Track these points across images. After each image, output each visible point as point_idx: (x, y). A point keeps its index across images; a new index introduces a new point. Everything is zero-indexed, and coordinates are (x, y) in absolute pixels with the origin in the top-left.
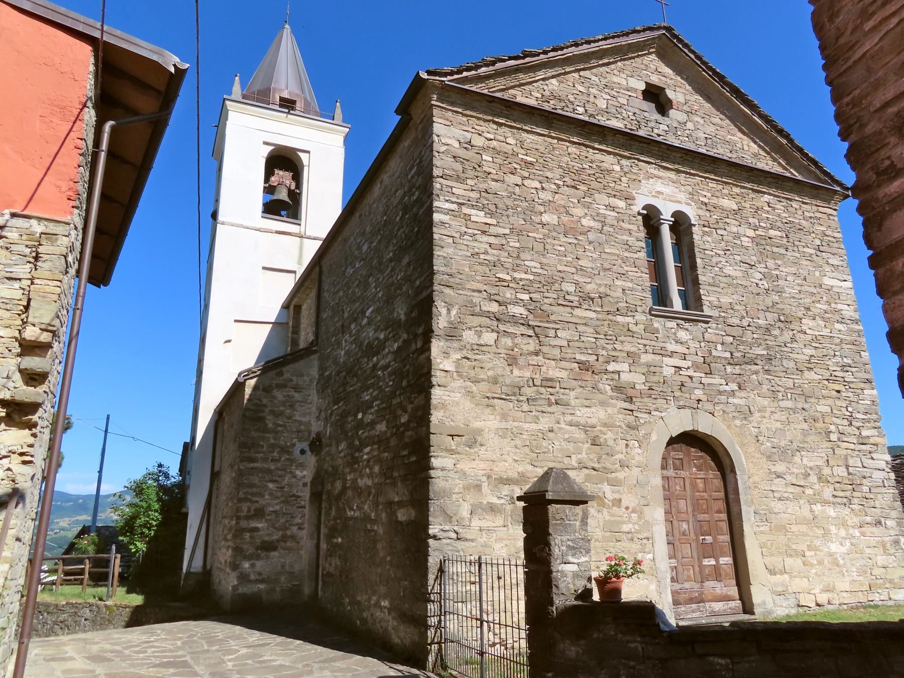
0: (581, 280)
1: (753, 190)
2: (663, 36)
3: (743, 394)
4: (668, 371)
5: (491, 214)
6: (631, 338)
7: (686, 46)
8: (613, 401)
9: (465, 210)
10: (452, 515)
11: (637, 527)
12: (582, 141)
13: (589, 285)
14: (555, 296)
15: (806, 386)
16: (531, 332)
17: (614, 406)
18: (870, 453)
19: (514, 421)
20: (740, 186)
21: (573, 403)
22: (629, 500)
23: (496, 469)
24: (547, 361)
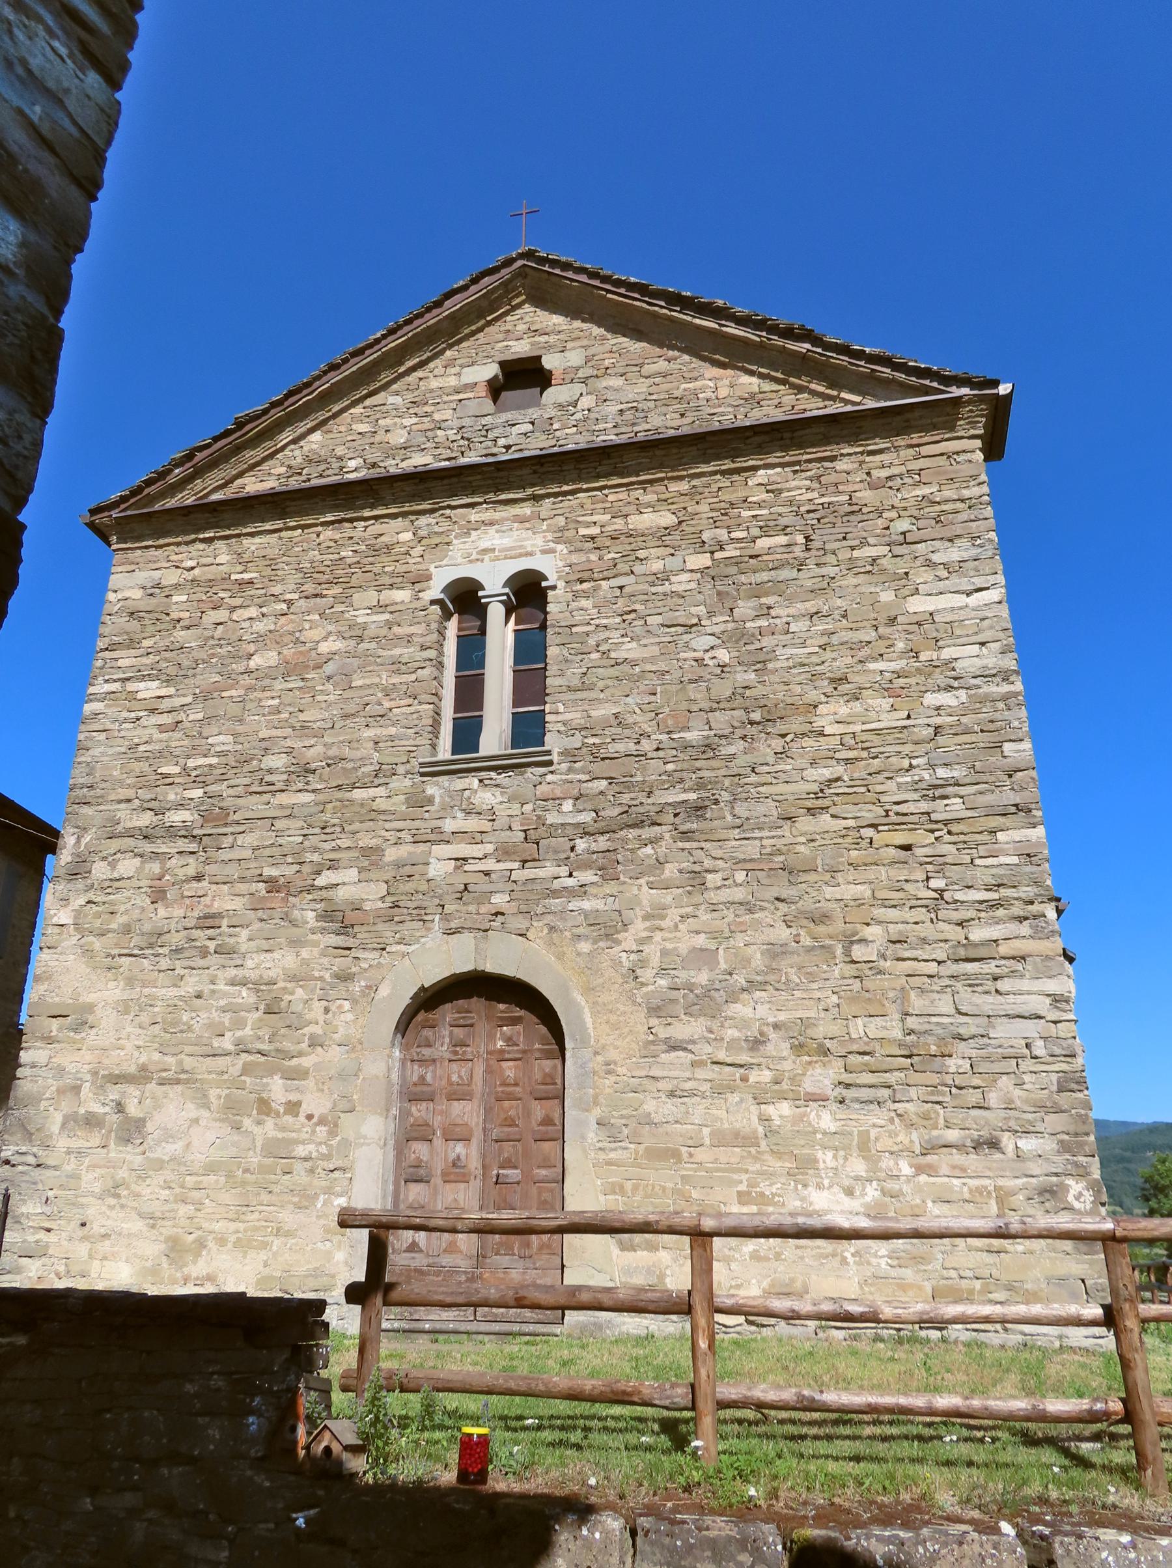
0: (298, 744)
1: (723, 473)
2: (527, 269)
3: (611, 888)
4: (438, 869)
5: (168, 682)
6: (371, 823)
7: (566, 266)
8: (314, 937)
9: (131, 686)
10: (33, 1131)
11: (323, 1149)
12: (342, 515)
13: (312, 750)
14: (247, 781)
15: (802, 848)
16: (193, 847)
17: (315, 944)
18: (995, 979)
19: (144, 986)
20: (688, 476)
21: (243, 948)
22: (315, 1102)
23: (106, 1061)
24: (214, 887)
